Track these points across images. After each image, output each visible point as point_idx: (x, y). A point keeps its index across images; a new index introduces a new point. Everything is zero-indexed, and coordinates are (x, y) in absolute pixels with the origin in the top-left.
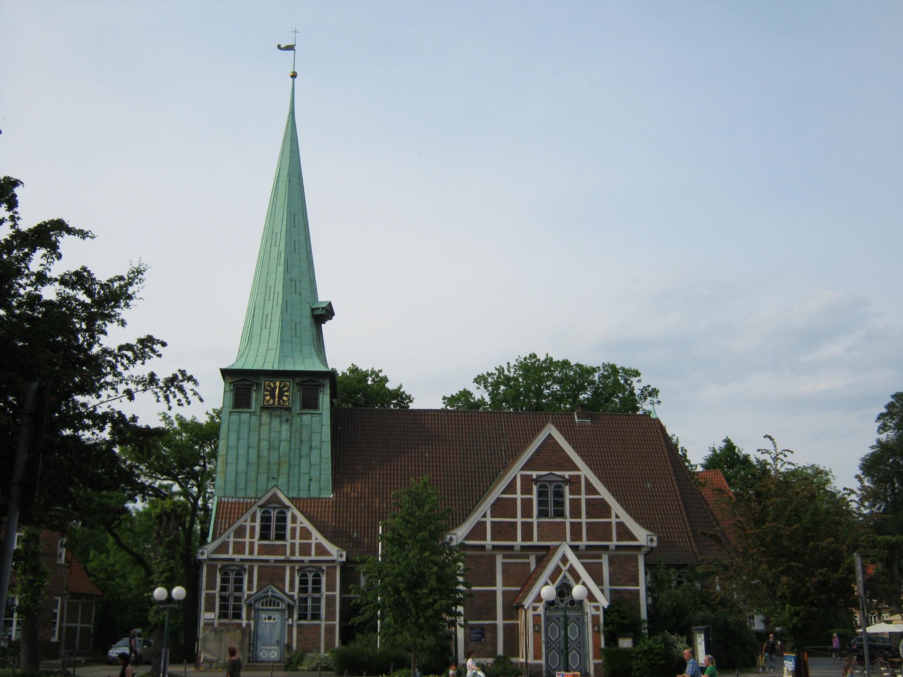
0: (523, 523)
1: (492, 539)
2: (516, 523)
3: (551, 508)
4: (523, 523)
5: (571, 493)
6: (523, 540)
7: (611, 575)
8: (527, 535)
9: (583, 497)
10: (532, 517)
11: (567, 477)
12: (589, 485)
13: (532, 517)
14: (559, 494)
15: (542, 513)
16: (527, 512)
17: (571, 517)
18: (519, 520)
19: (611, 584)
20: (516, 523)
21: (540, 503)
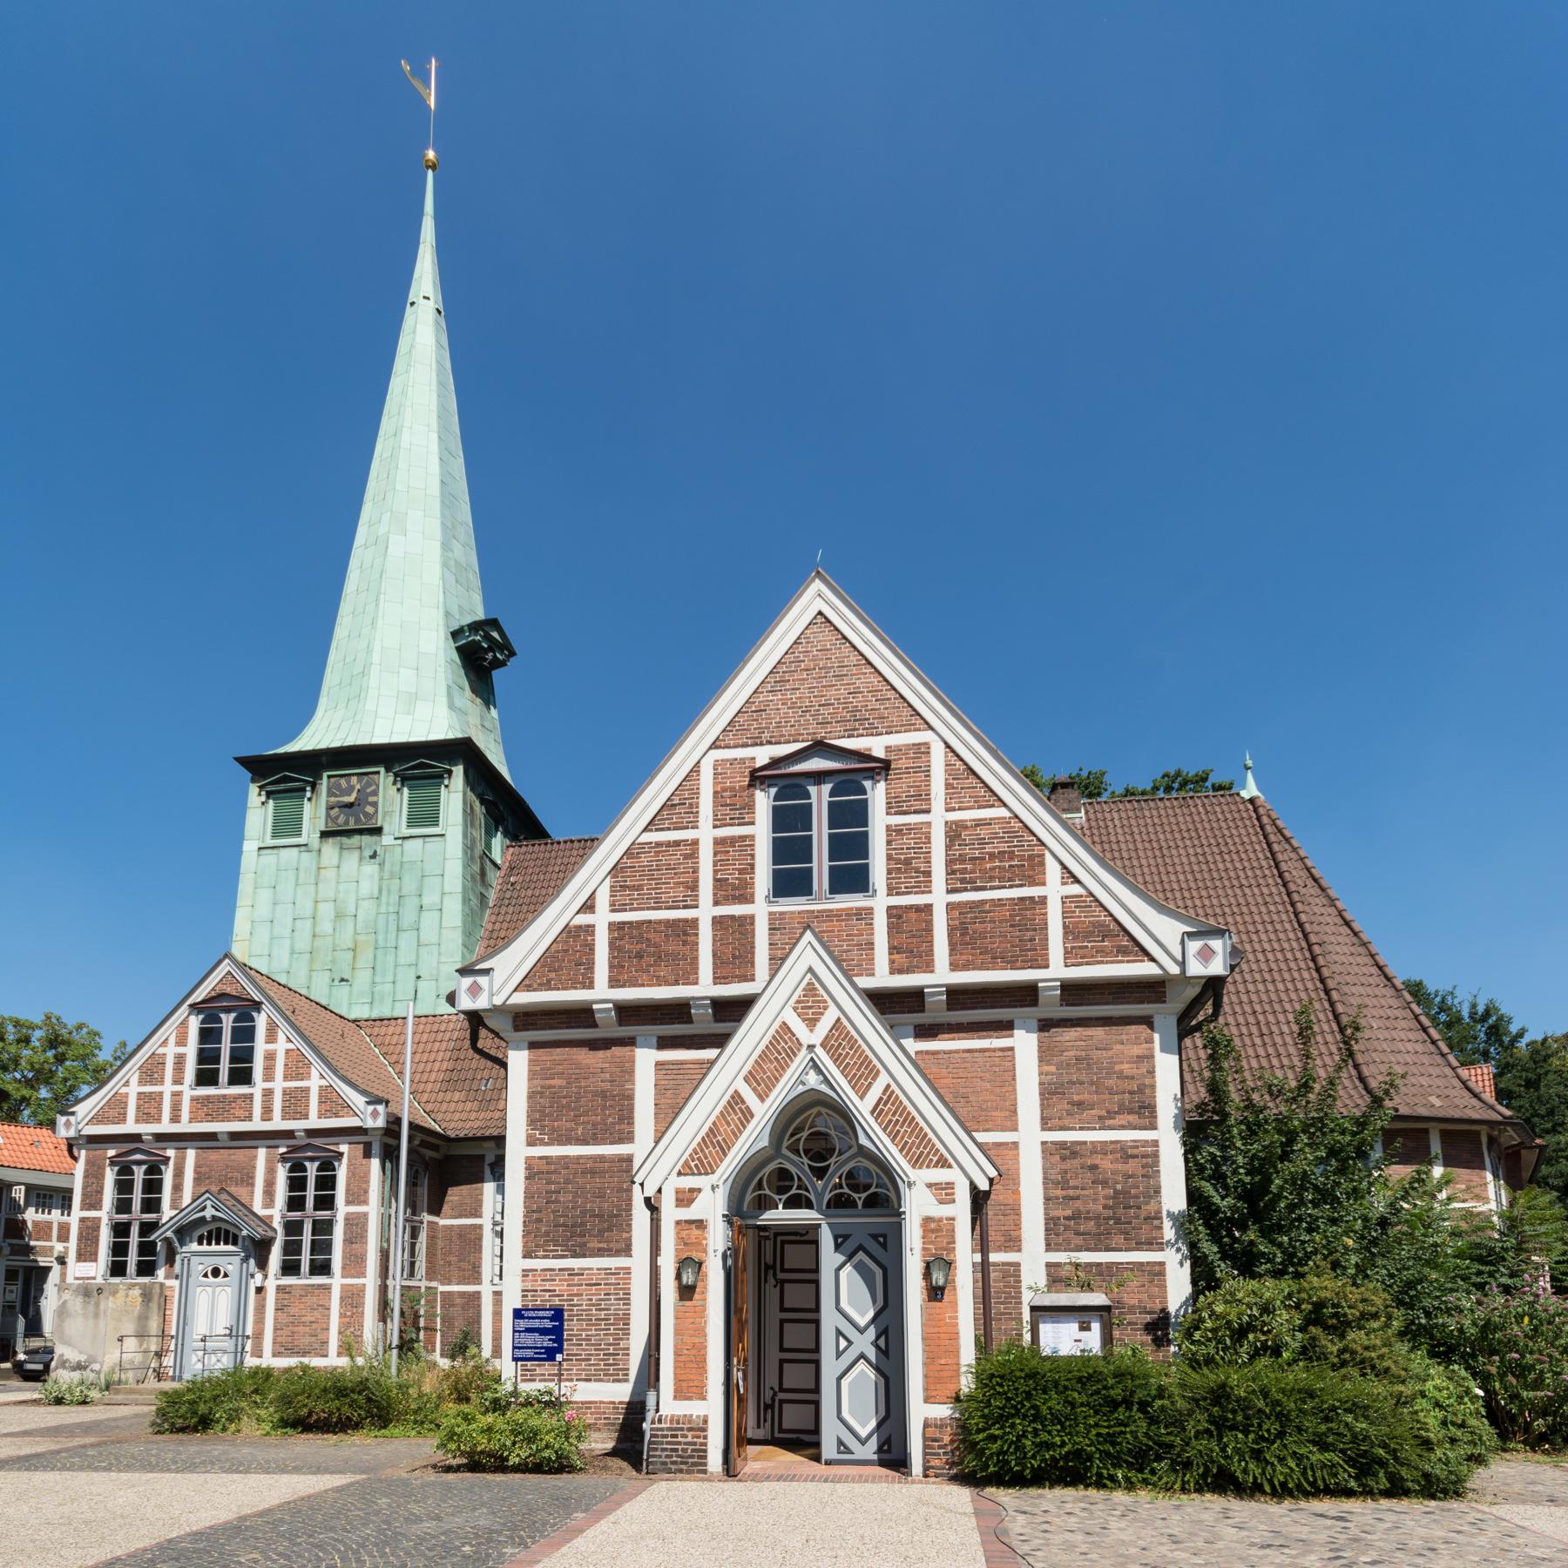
0: (718, 922)
1: (614, 983)
2: (694, 923)
3: (821, 864)
4: (718, 922)
5: (893, 807)
6: (717, 980)
7: (1049, 1092)
8: (734, 960)
9: (938, 818)
10: (749, 899)
11: (879, 753)
12: (963, 775)
13: (749, 899)
14: (850, 815)
15: (790, 883)
16: (733, 889)
17: (891, 891)
18: (705, 912)
19: (1046, 1124)
20: (694, 923)
21: (782, 851)
